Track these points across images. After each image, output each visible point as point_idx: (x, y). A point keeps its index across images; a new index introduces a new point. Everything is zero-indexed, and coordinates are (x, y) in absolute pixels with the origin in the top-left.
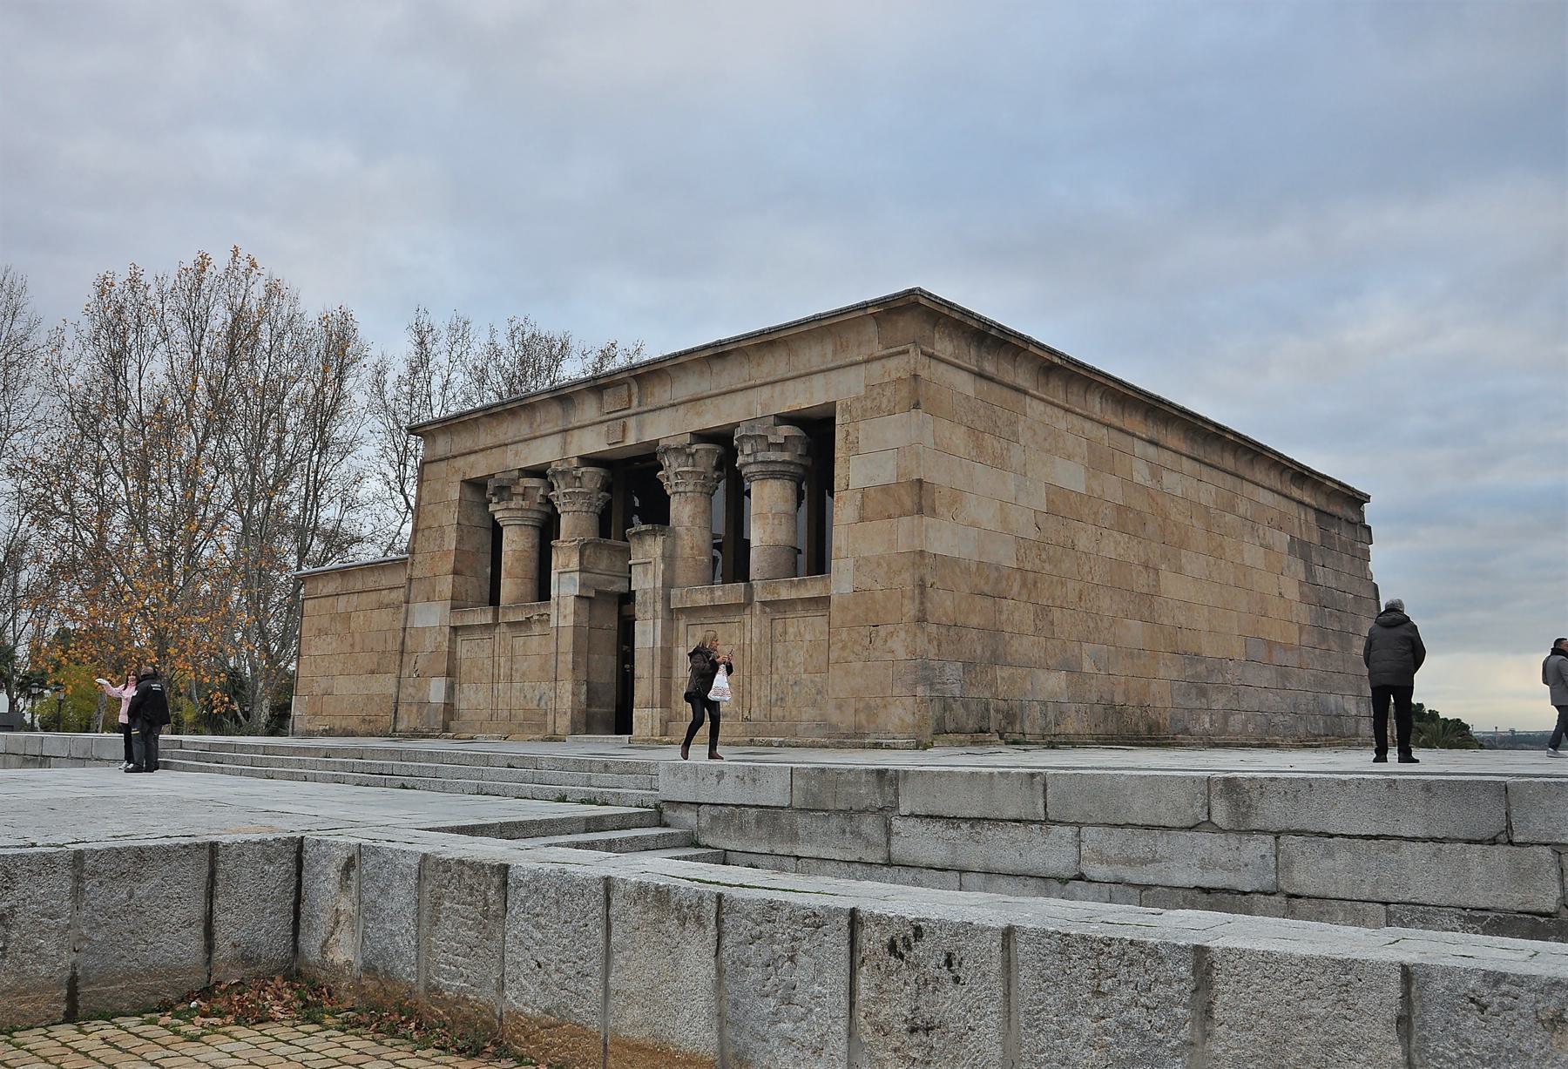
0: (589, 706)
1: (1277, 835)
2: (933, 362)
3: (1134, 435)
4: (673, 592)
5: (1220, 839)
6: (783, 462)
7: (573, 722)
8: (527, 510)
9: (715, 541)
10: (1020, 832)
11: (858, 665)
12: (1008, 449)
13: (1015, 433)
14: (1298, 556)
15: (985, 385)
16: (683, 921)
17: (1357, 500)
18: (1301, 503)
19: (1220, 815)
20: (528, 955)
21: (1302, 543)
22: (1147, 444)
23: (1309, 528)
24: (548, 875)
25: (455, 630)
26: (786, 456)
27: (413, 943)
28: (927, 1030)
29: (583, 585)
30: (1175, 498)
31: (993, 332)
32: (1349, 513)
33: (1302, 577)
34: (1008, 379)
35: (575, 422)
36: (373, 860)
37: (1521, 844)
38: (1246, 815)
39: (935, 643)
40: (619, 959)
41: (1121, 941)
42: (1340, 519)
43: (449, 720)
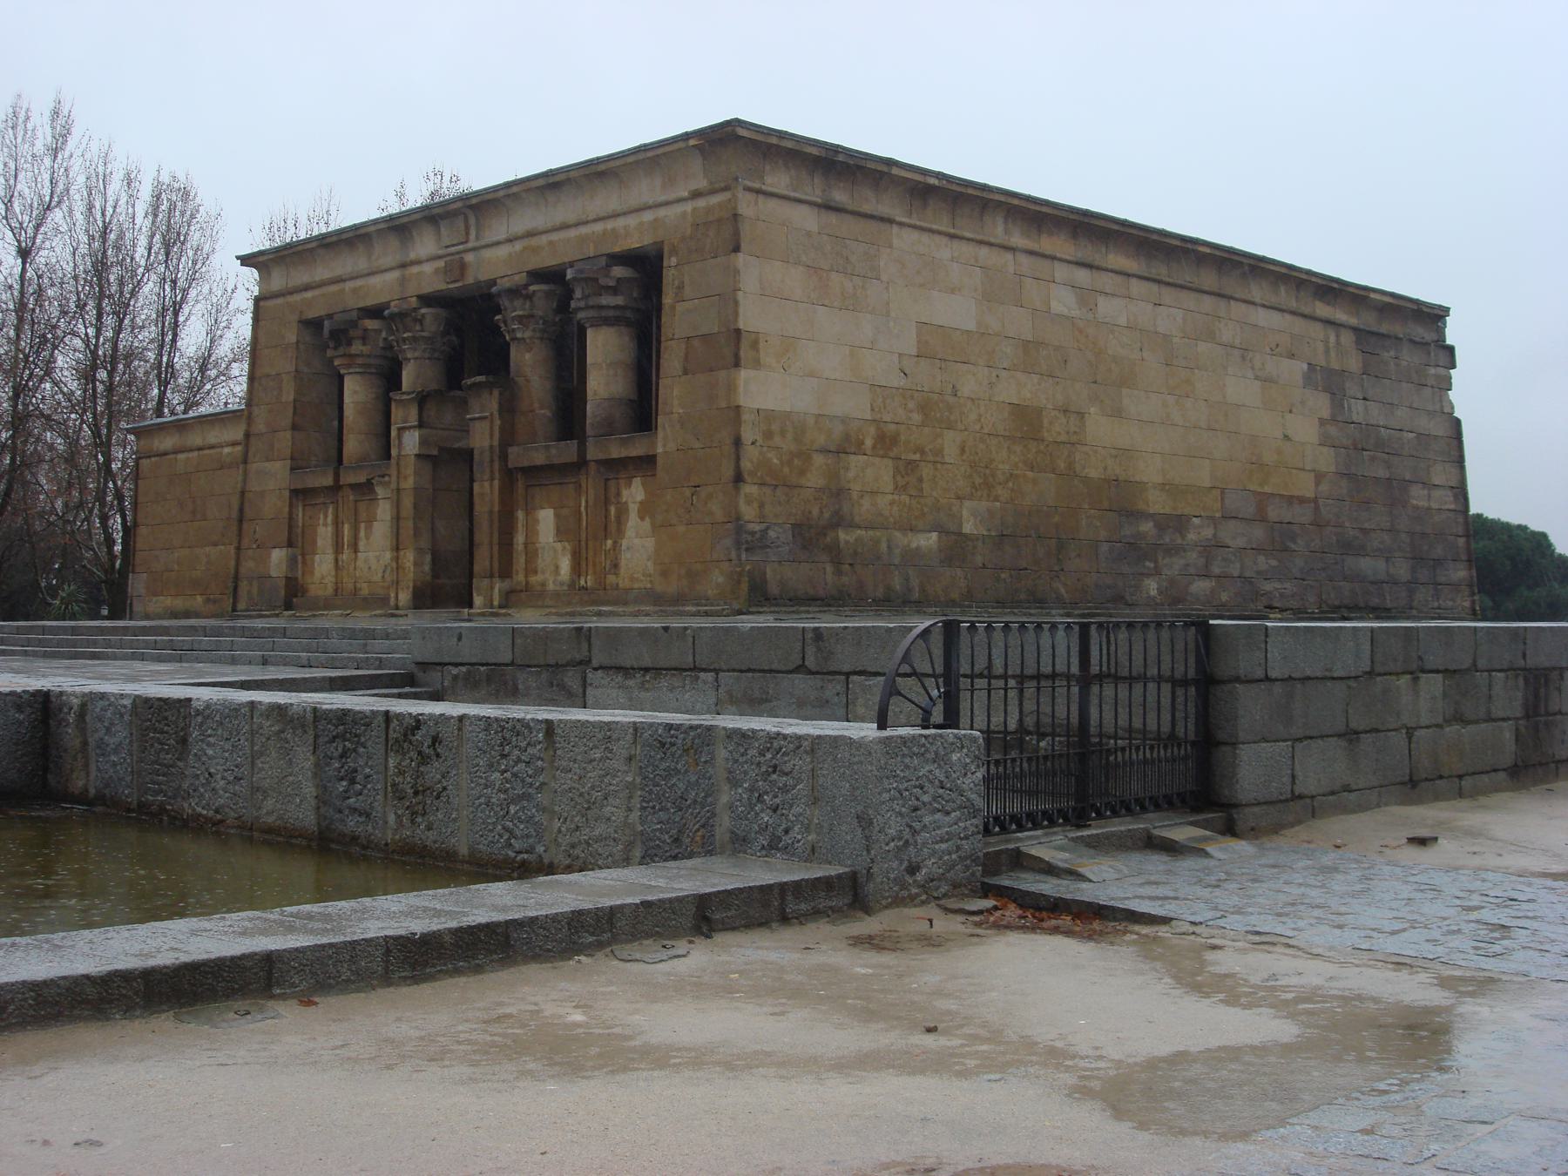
1: (848, 674)
2: (761, 198)
3: (1053, 258)
4: (510, 450)
6: (616, 307)
8: (369, 356)
11: (681, 529)
12: (863, 287)
14: (1320, 388)
15: (833, 218)
17: (1435, 316)
18: (1329, 322)
19: (811, 662)
20: (203, 768)
21: (1329, 373)
22: (1074, 266)
24: (216, 704)
25: (295, 493)
26: (619, 300)
29: (424, 442)
30: (1115, 328)
31: (841, 158)
32: (1421, 332)
33: (1326, 413)
34: (867, 208)
35: (412, 256)
36: (101, 704)
39: (756, 505)
42: (1401, 339)
43: (293, 595)
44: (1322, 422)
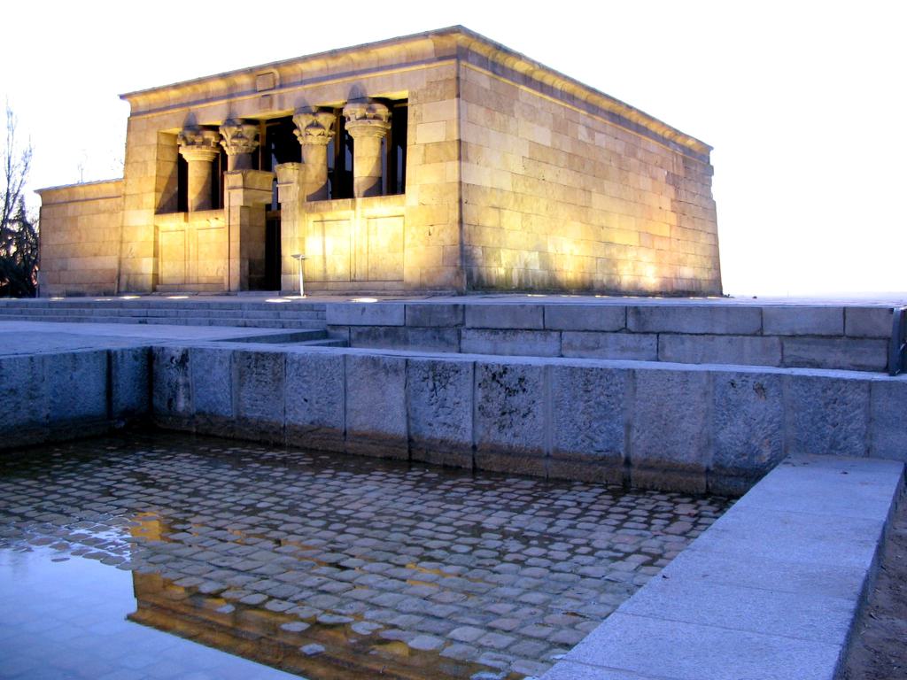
0: (250, 274)
1: (658, 334)
5: (631, 337)
7: (241, 283)
9: (384, 188)
10: (530, 336)
13: (512, 111)
16: (387, 373)
19: (631, 324)
23: (678, 166)
27: (229, 396)
28: (510, 413)
29: (246, 199)
33: (673, 197)
37: (768, 336)
38: (643, 325)
40: (352, 394)
41: (597, 368)
44: (672, 201)
